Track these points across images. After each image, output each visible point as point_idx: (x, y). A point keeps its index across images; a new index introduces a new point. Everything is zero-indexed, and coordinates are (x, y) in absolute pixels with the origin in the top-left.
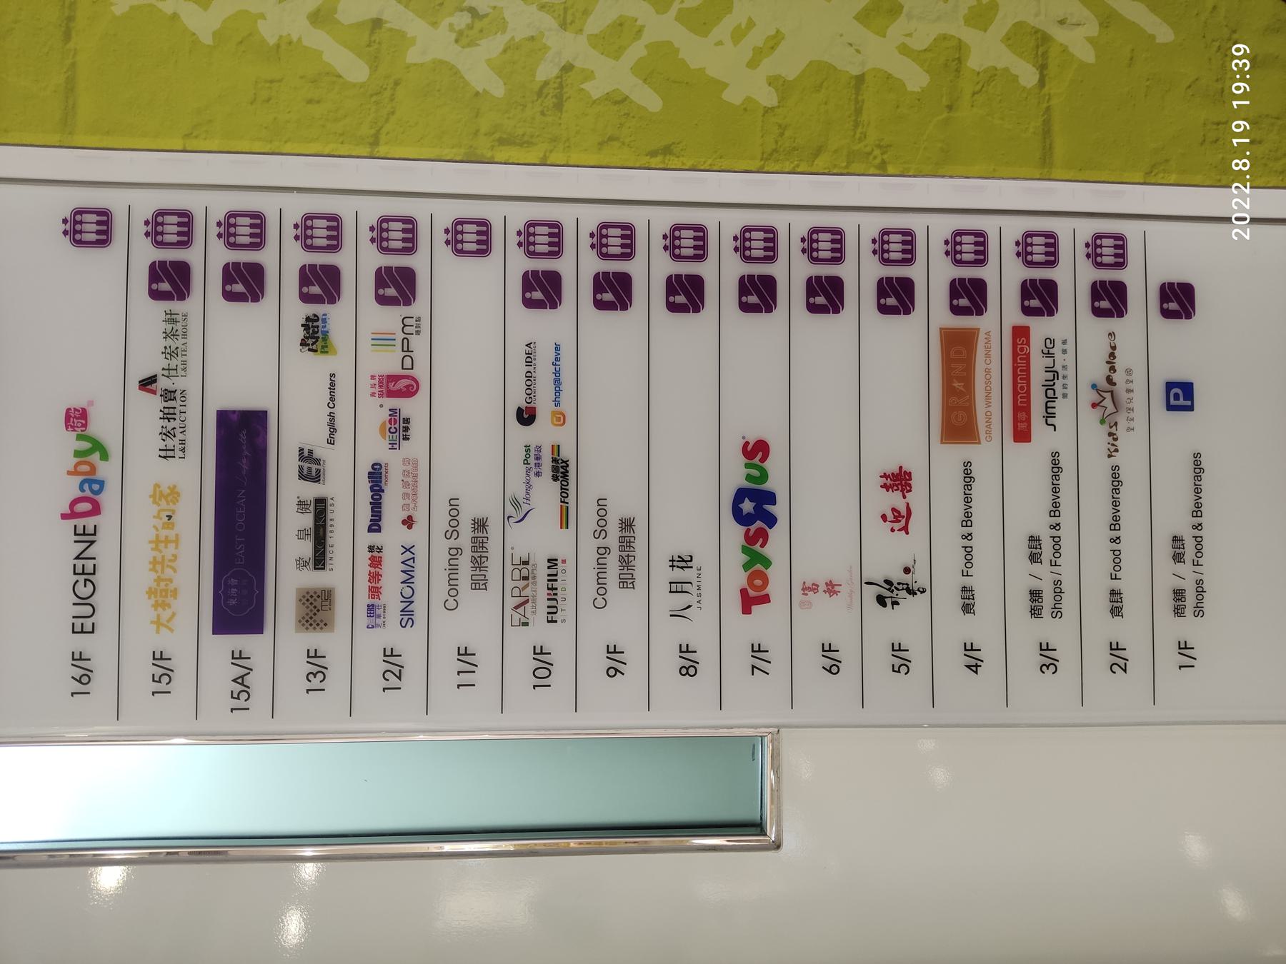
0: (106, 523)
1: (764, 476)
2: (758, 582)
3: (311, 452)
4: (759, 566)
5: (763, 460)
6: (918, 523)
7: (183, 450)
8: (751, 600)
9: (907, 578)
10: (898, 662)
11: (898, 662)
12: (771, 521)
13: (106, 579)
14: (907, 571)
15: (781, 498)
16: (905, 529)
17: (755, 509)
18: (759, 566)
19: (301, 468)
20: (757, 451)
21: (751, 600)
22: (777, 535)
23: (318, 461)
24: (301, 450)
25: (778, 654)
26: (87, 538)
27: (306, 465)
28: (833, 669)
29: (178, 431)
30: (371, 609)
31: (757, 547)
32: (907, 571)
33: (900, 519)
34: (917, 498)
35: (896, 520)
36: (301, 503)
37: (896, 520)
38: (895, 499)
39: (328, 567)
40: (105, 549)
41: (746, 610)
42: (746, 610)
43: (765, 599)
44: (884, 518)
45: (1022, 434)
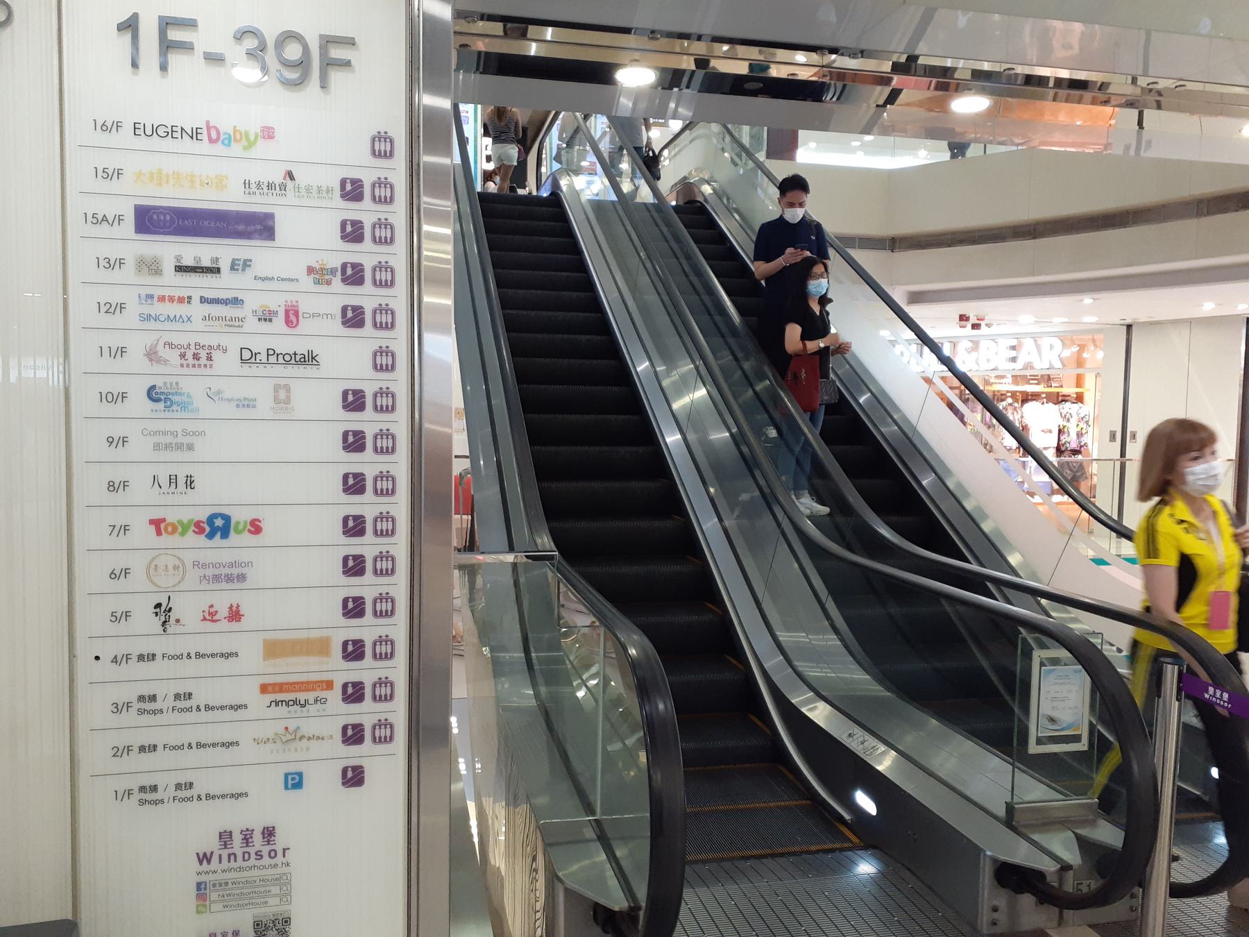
0: (204, 147)
1: (238, 532)
2: (170, 529)
4: (180, 529)
5: (249, 531)
6: (209, 626)
8: (157, 524)
9: (172, 620)
10: (118, 615)
11: (118, 615)
12: (211, 536)
13: (168, 144)
14: (178, 621)
15: (224, 543)
16: (205, 619)
17: (217, 526)
18: (180, 529)
20: (255, 527)
21: (157, 524)
22: (202, 540)
23: (243, 270)
25: (123, 541)
26: (195, 135)
28: (113, 575)
30: (151, 297)
31: (193, 528)
32: (178, 621)
33: (211, 616)
34: (224, 625)
35: (210, 614)
37: (210, 614)
38: (224, 612)
40: (187, 144)
41: (152, 522)
42: (152, 522)
43: (159, 533)
44: (212, 606)
45: (264, 689)
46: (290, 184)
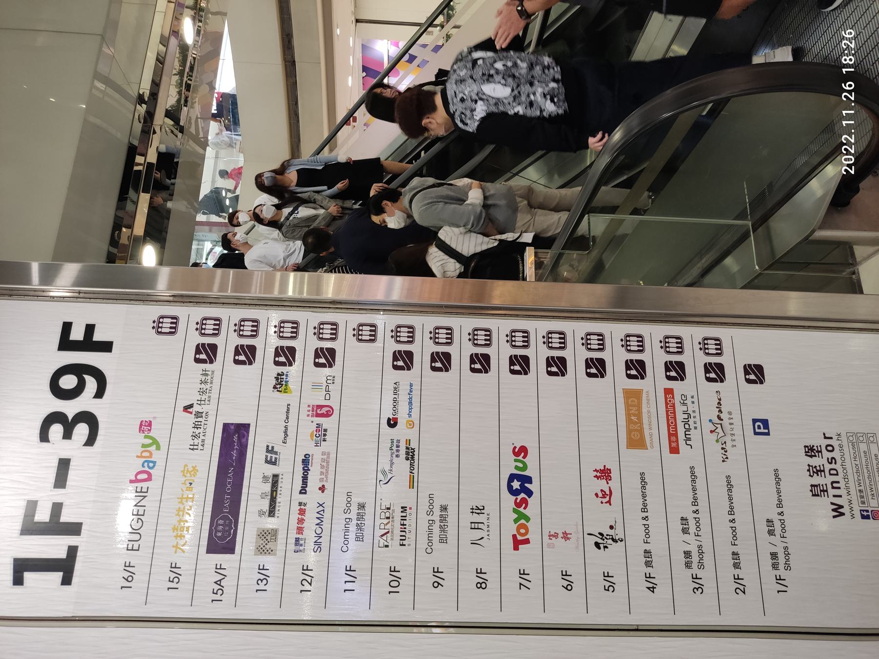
3: (273, 447)
7: (203, 445)
19: (267, 456)
23: (276, 453)
24: (268, 446)
27: (269, 455)
29: (202, 434)
36: (264, 477)
39: (276, 515)
46: (197, 408)
